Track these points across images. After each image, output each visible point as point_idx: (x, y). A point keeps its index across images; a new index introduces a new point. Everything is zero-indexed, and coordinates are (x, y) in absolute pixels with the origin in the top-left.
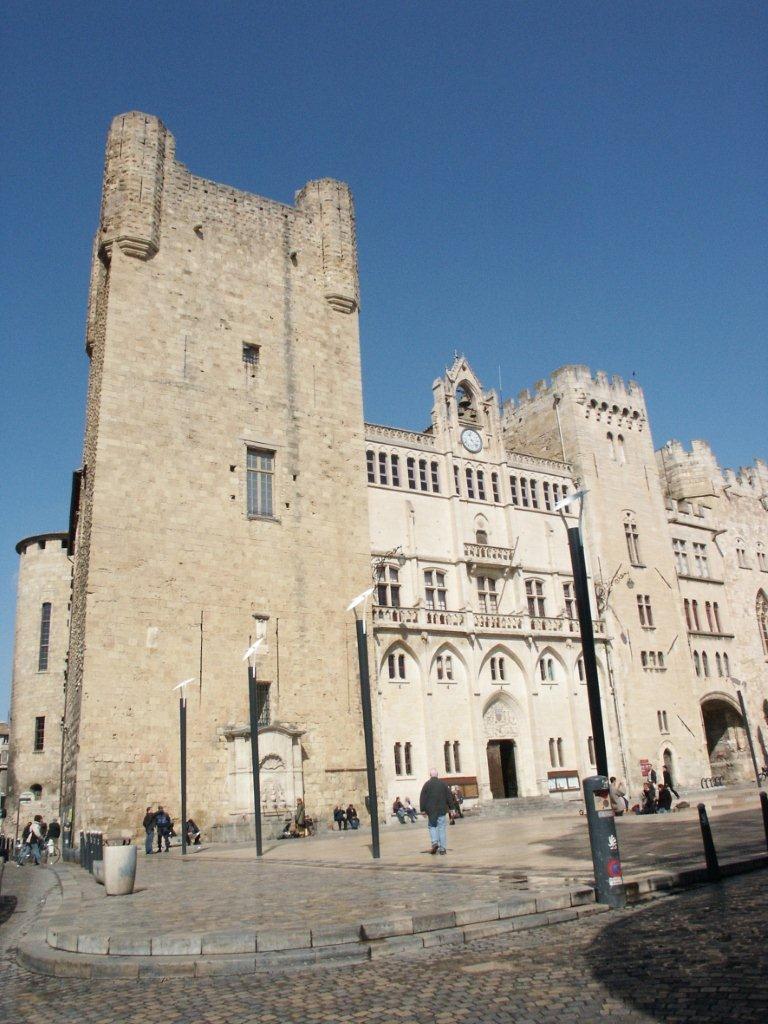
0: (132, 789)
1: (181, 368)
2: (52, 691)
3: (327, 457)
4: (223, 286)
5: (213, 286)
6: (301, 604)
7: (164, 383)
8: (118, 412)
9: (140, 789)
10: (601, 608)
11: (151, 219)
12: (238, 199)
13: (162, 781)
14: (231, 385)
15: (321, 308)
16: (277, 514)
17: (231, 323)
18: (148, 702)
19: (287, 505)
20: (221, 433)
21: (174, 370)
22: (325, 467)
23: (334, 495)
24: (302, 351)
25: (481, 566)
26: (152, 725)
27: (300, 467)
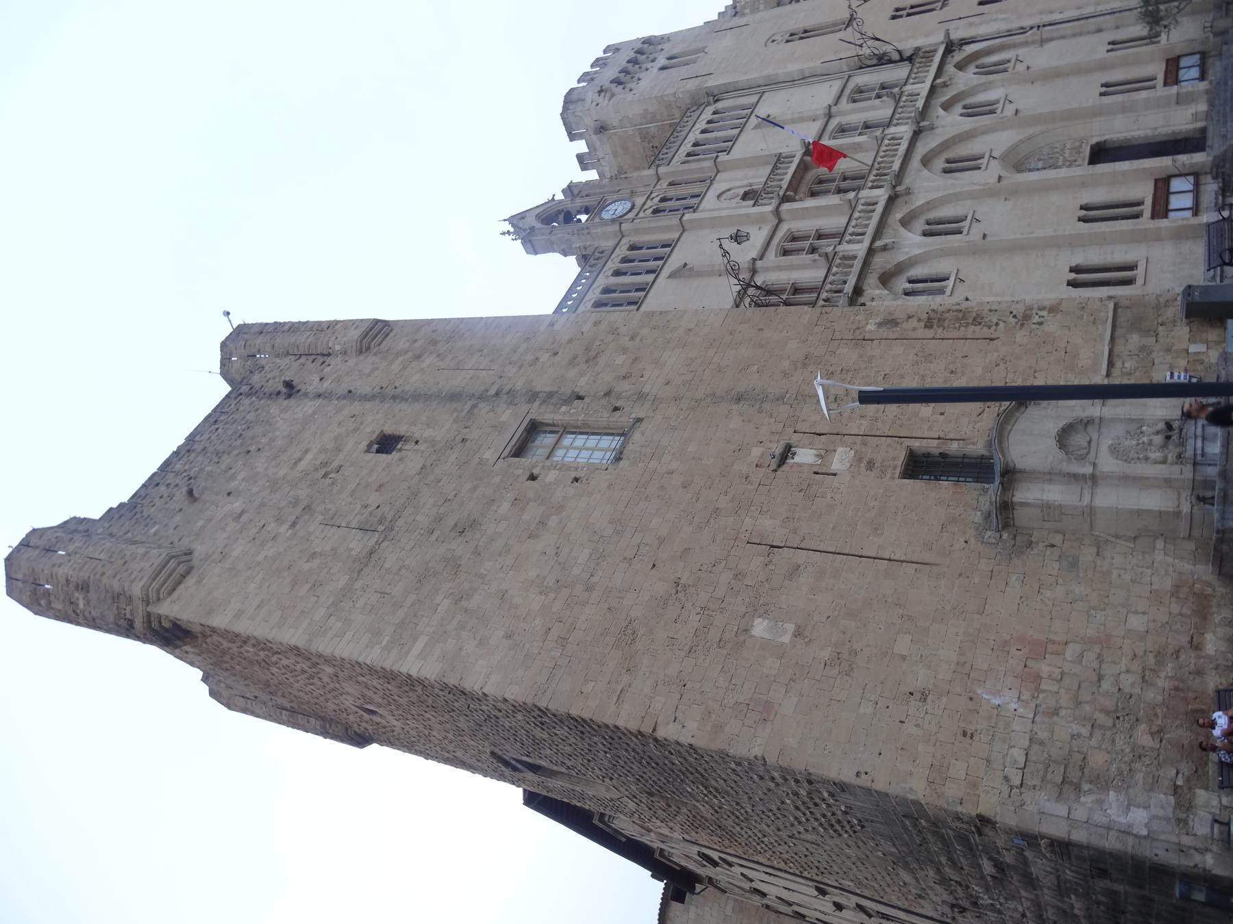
0: (1101, 718)
1: (360, 534)
6: (780, 399)
9: (1109, 704)
10: (896, 56)
13: (1090, 656)
15: (371, 359)
17: (334, 465)
18: (904, 658)
19: (616, 409)
20: (475, 488)
21: (358, 544)
23: (624, 351)
24: (414, 380)
27: (567, 391)
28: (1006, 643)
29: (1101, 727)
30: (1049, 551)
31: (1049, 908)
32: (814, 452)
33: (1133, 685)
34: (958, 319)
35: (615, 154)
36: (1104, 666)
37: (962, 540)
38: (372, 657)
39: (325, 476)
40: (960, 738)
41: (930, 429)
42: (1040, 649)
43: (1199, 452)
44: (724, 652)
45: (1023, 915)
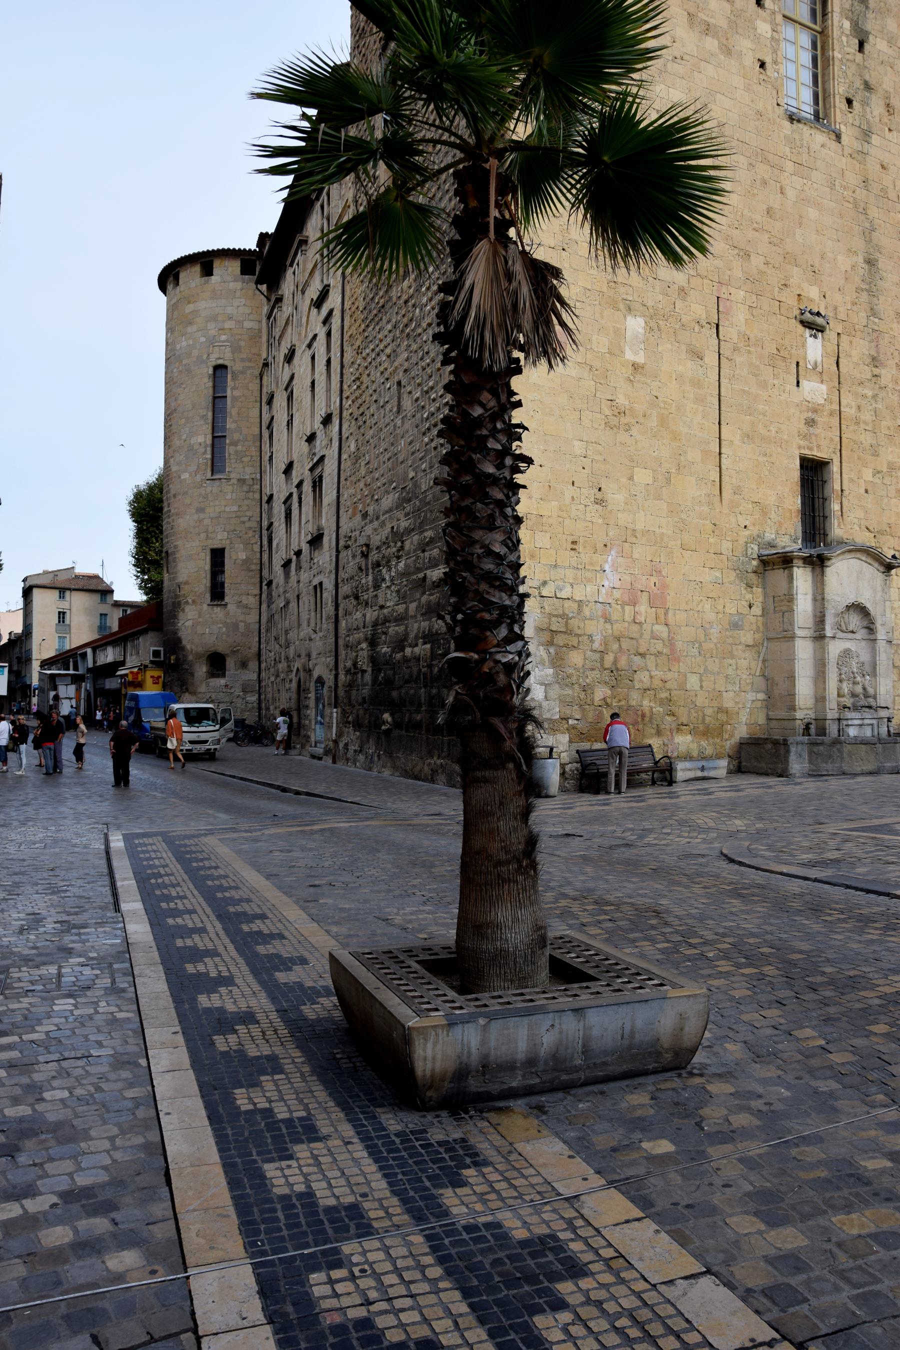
0: (609, 659)
2: (235, 508)
6: (873, 312)
9: (623, 663)
13: (659, 646)
18: (631, 478)
26: (639, 526)
28: (659, 572)
29: (602, 659)
30: (746, 604)
31: (403, 628)
32: (819, 360)
33: (641, 681)
36: (652, 657)
37: (747, 523)
40: (571, 539)
41: (851, 480)
42: (657, 601)
43: (850, 722)
44: (605, 289)
45: (382, 607)
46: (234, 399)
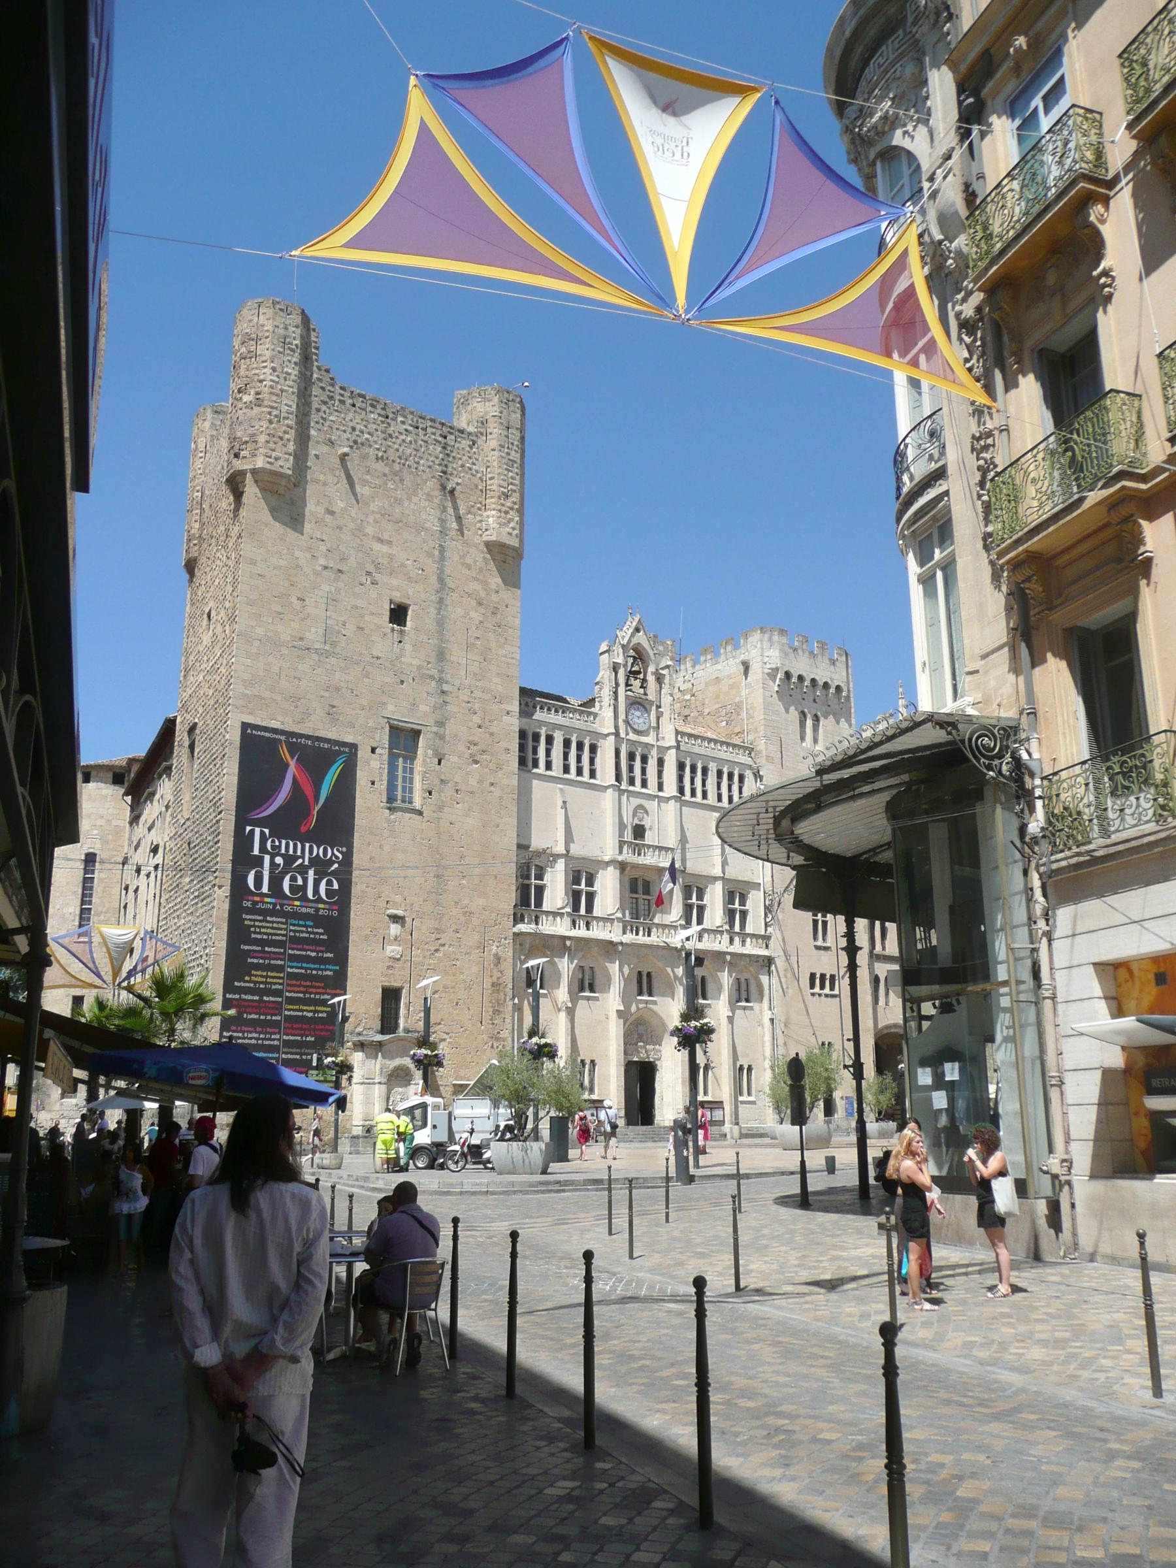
1: (321, 631)
3: (471, 739)
4: (370, 530)
5: (359, 531)
7: (301, 648)
8: (250, 683)
11: (291, 447)
12: (391, 415)
14: (375, 653)
16: (417, 803)
17: (378, 577)
19: (430, 793)
21: (314, 635)
22: (474, 749)
23: (480, 782)
24: (455, 612)
25: (635, 866)
34: (498, 1001)
35: (729, 677)
38: (237, 688)
39: (369, 573)
46: (101, 880)
